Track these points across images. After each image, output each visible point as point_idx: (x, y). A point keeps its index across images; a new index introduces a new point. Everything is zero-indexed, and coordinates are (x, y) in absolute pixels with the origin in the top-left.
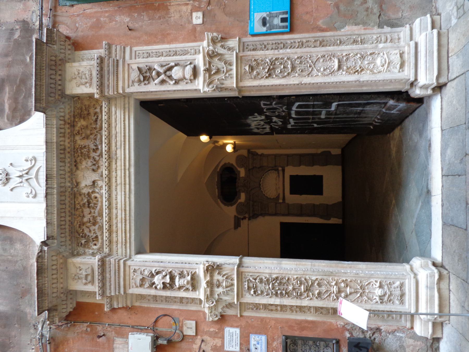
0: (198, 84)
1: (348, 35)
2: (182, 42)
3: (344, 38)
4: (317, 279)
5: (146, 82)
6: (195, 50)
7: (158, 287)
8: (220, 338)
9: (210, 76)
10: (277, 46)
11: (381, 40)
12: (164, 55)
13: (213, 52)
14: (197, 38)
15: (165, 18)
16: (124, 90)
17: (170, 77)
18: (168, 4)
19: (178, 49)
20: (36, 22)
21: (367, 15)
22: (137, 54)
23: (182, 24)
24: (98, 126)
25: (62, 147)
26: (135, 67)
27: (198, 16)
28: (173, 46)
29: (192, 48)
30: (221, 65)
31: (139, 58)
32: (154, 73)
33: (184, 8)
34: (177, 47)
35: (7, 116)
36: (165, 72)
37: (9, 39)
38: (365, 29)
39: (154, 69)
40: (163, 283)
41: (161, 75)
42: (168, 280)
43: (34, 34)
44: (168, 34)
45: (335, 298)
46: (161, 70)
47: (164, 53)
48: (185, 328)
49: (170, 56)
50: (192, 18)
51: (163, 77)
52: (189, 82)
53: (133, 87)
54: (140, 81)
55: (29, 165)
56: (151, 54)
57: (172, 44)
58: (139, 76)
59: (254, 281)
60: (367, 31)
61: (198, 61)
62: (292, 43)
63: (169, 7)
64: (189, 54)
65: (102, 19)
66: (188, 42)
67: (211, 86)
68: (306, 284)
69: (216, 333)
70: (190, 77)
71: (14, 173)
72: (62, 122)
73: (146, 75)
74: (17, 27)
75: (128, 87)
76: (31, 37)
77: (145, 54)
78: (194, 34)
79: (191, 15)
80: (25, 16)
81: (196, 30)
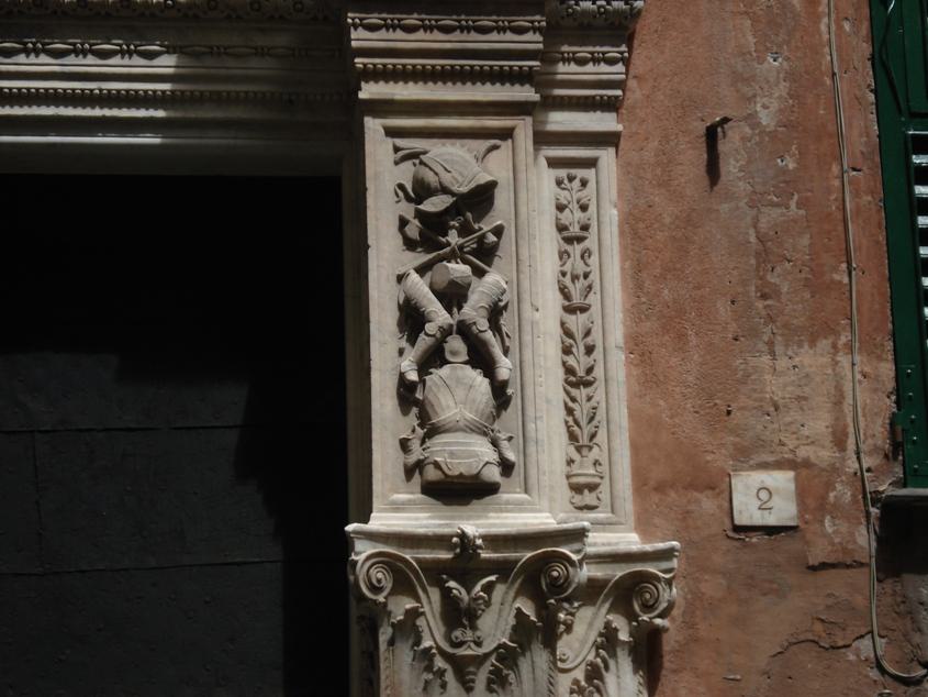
0: (397, 507)
2: (634, 415)
5: (414, 230)
6: (592, 487)
9: (435, 572)
12: (571, 320)
13: (558, 587)
14: (656, 498)
15: (771, 319)
16: (381, 108)
17: (434, 358)
18: (843, 339)
19: (600, 396)
22: (580, 173)
23: (736, 414)
26: (497, 167)
27: (776, 502)
28: (615, 367)
29: (604, 468)
30: (495, 628)
31: (559, 183)
32: (459, 269)
34: (613, 388)
36: (464, 330)
39: (479, 273)
41: (449, 310)
44: (681, 336)
46: (474, 311)
47: (582, 317)
49: (567, 351)
50: (764, 466)
51: (439, 316)
52: (412, 459)
53: (391, 156)
54: (421, 191)
56: (577, 249)
57: (629, 363)
58: (445, 190)
61: (519, 507)
63: (824, 344)
66: (636, 448)
67: (378, 574)
70: (437, 465)
73: (456, 224)
75: (391, 132)
77: (578, 214)
78: (677, 478)
79: (779, 465)
81: (699, 489)
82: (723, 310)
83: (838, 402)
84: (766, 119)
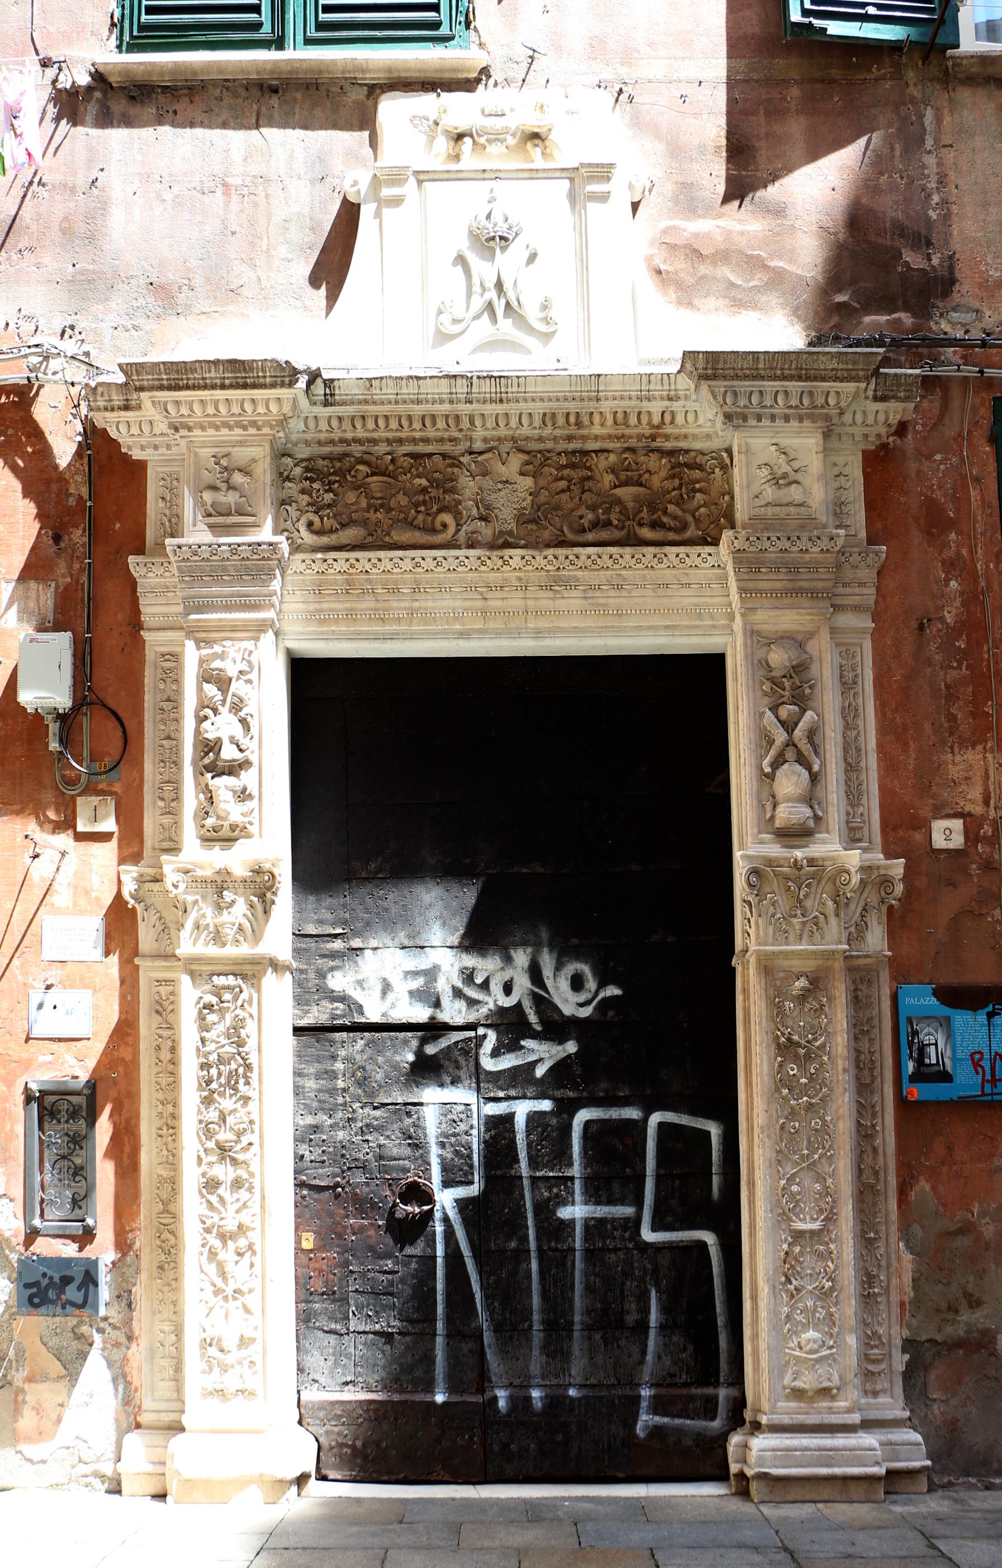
1: (889, 1258)
2: (882, 789)
3: (882, 1250)
4: (252, 1175)
7: (206, 725)
8: (75, 905)
10: (863, 1067)
11: (872, 1348)
19: (863, 777)
20: (949, 322)
21: (938, 1311)
23: (934, 789)
24: (646, 533)
25: (586, 420)
27: (954, 836)
29: (866, 818)
33: (976, 793)
34: (870, 773)
35: (674, 228)
37: (901, 231)
38: (902, 1304)
40: (218, 741)
42: (228, 753)
43: (915, 315)
44: (906, 744)
45: (209, 1222)
47: (854, 733)
48: (95, 800)
50: (948, 816)
55: (532, 313)
57: (879, 759)
59: (239, 1003)
60: (896, 1310)
62: (873, 1106)
64: (849, 808)
65: (953, 536)
66: (881, 806)
68: (238, 1147)
69: (87, 893)
71: (508, 262)
72: (656, 420)
74: (935, 261)
76: (906, 308)
80: (965, 289)
82: (927, 727)
83: (987, 777)
84: (949, 619)
